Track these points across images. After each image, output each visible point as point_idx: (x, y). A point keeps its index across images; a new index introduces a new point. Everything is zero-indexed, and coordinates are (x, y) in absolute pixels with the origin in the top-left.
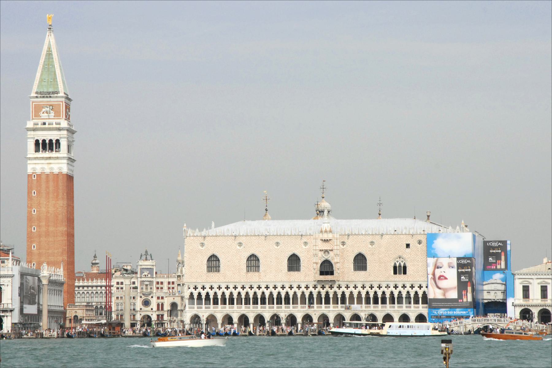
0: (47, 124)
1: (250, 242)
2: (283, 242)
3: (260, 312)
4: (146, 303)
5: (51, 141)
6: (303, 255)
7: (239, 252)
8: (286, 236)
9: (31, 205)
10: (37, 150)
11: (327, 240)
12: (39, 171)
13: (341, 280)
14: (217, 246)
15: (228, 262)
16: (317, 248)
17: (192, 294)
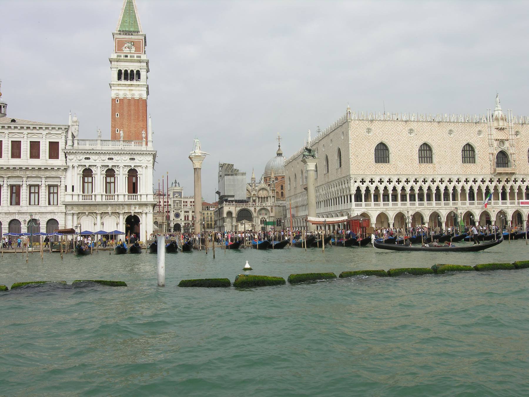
0: (129, 56)
1: (422, 129)
2: (457, 130)
3: (436, 209)
4: (177, 215)
5: (132, 71)
6: (478, 145)
7: (410, 140)
8: (460, 124)
9: (115, 126)
10: (119, 78)
11: (504, 128)
12: (121, 96)
13: (518, 173)
14: (386, 133)
15: (399, 151)
16: (493, 138)
17: (358, 190)
